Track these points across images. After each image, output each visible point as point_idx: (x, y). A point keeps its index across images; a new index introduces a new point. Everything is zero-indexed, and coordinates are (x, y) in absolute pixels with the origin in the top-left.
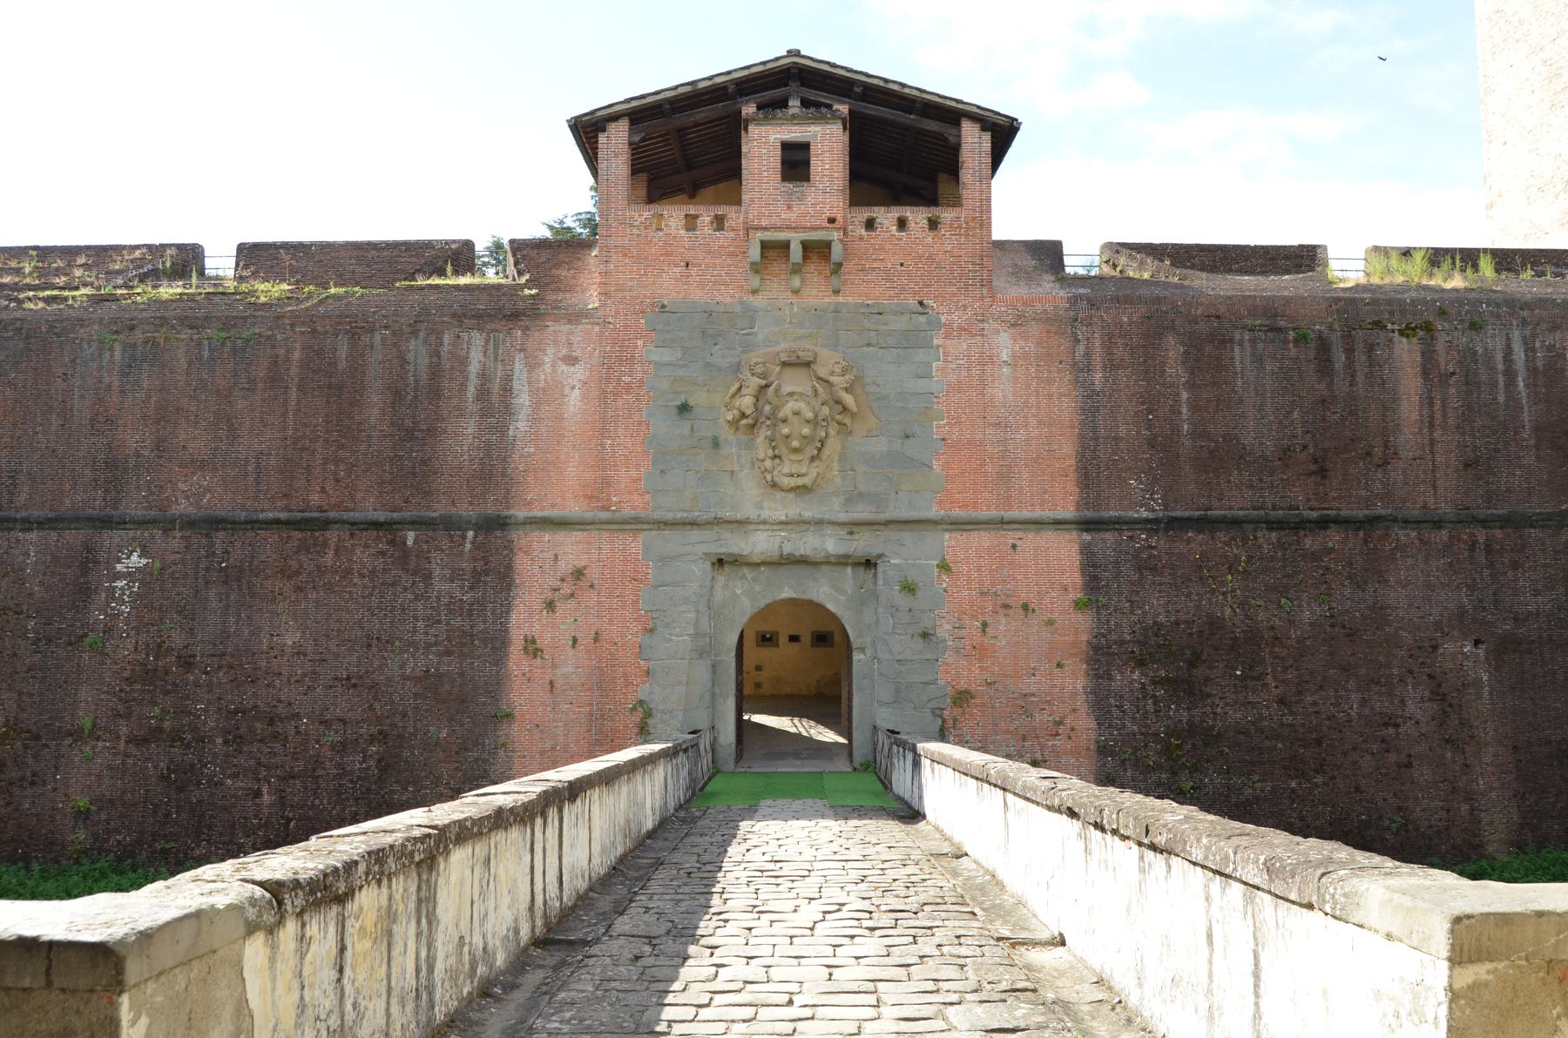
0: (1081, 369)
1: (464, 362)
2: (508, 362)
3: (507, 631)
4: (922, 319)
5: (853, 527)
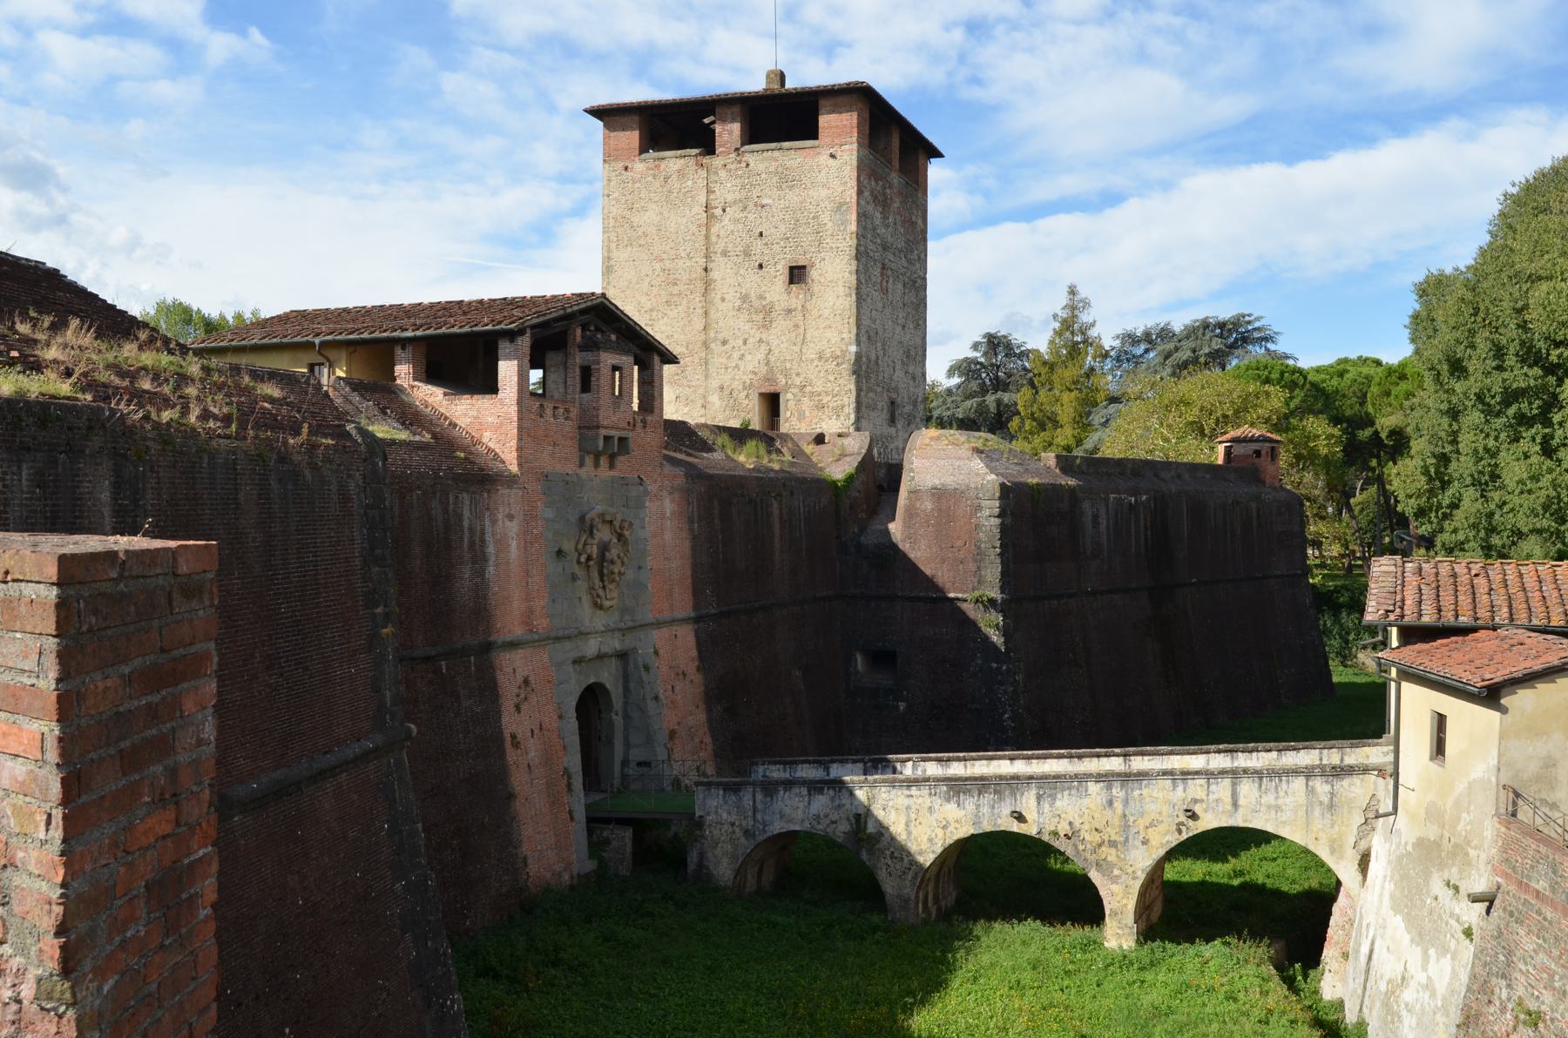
0: (691, 521)
1: (460, 517)
2: (482, 519)
3: (502, 732)
4: (641, 488)
5: (624, 631)
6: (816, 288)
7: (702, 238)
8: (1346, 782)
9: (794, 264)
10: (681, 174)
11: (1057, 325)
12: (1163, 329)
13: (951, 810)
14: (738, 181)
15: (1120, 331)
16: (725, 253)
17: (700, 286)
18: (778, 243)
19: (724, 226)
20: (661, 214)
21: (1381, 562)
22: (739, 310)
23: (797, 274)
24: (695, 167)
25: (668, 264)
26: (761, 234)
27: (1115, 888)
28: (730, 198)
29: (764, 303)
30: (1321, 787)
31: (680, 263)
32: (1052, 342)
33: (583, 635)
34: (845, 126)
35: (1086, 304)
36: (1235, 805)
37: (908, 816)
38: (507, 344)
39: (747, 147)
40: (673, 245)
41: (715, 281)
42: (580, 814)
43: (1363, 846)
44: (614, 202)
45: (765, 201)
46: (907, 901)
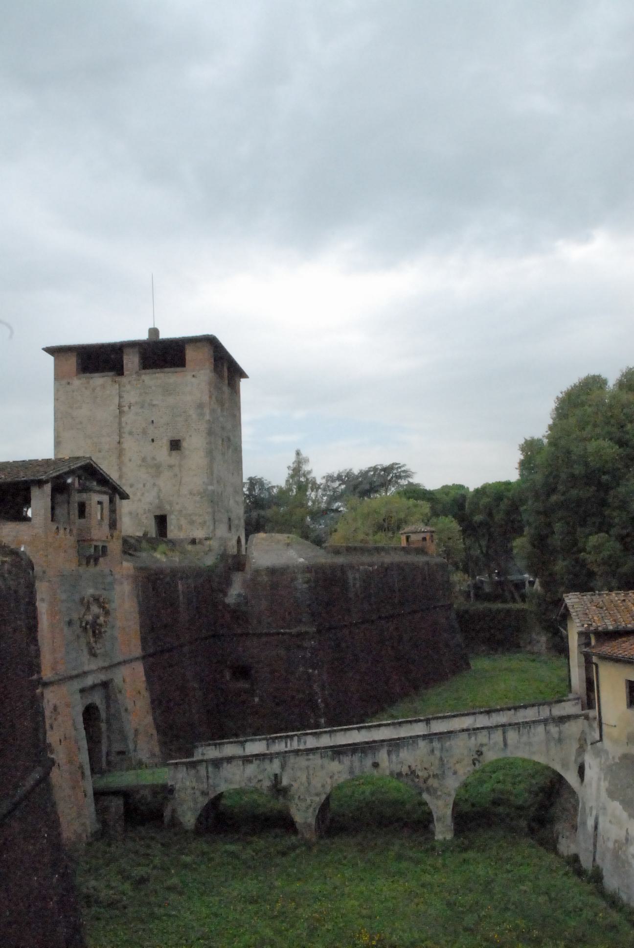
0: (138, 596)
8: (567, 725)
9: (173, 439)
10: (103, 386)
11: (291, 472)
12: (348, 473)
13: (334, 766)
15: (325, 475)
16: (131, 433)
18: (162, 427)
19: (129, 418)
21: (570, 597)
23: (175, 445)
26: (153, 421)
27: (440, 803)
28: (133, 400)
30: (554, 730)
32: (287, 481)
33: (85, 674)
35: (307, 461)
36: (505, 744)
37: (308, 772)
39: (144, 371)
41: (125, 449)
42: (90, 792)
43: (580, 760)
45: (155, 402)
46: (309, 825)
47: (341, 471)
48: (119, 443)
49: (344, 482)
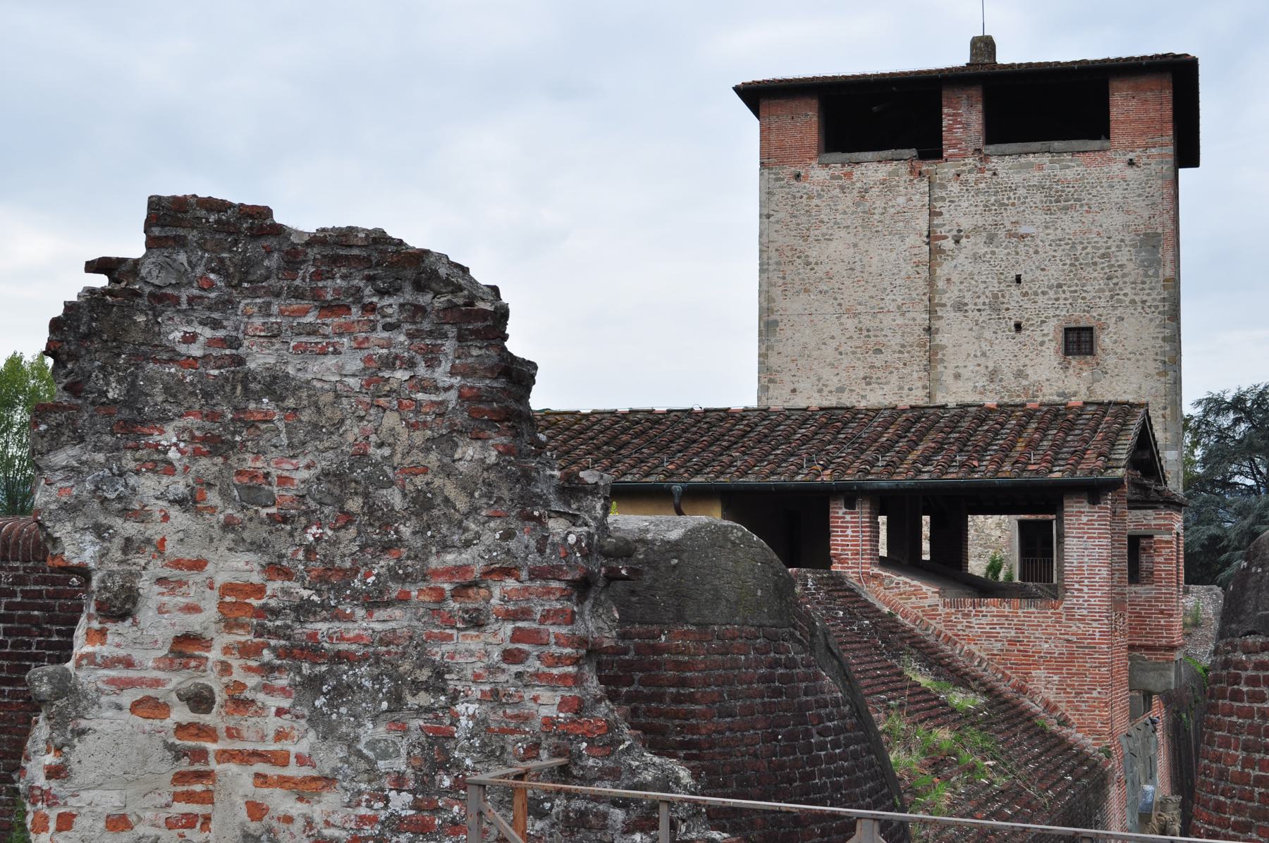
6: (1111, 361)
7: (921, 282)
9: (1073, 325)
14: (982, 198)
15: (1203, 395)
16: (960, 307)
17: (921, 357)
18: (1044, 293)
20: (855, 245)
22: (981, 393)
24: (907, 177)
25: (867, 322)
26: (1018, 279)
28: (966, 224)
29: (1025, 383)
31: (887, 320)
34: (1152, 120)
38: (1086, 507)
39: (992, 148)
40: (872, 292)
41: (943, 347)
44: (778, 227)
45: (1023, 230)
47: (1244, 389)
48: (929, 330)
49: (1249, 415)
